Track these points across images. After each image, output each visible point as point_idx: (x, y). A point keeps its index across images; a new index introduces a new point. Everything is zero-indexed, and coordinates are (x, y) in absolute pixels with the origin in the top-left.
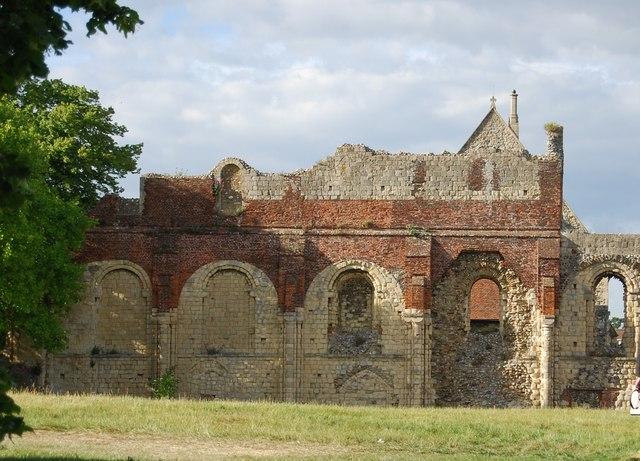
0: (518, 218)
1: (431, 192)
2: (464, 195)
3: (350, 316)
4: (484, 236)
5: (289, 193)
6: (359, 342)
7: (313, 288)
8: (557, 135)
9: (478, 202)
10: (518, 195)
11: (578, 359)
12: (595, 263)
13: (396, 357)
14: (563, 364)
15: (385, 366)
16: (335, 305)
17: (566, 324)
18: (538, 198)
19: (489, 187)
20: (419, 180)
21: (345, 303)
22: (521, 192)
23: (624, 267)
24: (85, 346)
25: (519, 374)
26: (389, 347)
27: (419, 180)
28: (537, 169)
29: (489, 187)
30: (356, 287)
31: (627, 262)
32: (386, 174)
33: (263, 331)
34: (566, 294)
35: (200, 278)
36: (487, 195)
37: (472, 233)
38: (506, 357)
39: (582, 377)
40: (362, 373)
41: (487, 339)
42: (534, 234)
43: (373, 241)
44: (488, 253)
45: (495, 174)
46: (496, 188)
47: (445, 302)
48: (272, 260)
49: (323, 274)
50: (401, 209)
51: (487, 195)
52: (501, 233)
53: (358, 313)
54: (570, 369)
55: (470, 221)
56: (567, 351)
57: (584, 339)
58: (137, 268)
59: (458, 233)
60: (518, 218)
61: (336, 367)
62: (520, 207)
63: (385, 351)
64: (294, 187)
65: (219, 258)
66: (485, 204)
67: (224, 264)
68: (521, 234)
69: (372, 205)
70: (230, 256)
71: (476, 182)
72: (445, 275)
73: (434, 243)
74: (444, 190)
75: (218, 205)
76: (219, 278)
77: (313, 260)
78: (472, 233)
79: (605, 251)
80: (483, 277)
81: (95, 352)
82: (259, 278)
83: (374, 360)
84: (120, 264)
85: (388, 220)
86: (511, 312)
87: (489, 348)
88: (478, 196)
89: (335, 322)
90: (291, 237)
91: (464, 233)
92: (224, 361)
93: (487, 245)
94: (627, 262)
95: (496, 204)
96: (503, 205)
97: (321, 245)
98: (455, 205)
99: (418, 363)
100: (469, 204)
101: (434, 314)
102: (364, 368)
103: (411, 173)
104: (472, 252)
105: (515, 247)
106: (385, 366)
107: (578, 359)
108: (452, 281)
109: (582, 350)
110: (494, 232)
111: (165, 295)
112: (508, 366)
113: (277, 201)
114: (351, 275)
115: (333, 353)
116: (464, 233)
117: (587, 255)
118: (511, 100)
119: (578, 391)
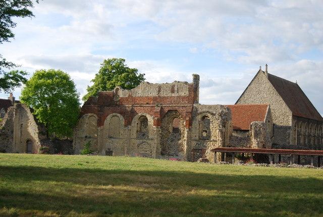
1: (163, 94)
2: (170, 95)
4: (174, 106)
6: (144, 135)
7: (133, 121)
8: (196, 78)
10: (183, 94)
12: (201, 113)
13: (152, 139)
15: (149, 142)
16: (139, 125)
17: (193, 130)
19: (176, 92)
20: (159, 91)
24: (84, 136)
25: (181, 144)
26: (150, 137)
27: (159, 91)
28: (188, 87)
29: (176, 92)
30: (144, 120)
31: (209, 113)
33: (122, 132)
35: (109, 117)
36: (175, 95)
38: (179, 140)
41: (175, 134)
46: (178, 93)
47: (164, 124)
48: (123, 113)
49: (136, 117)
50: (155, 99)
51: (175, 95)
53: (146, 127)
54: (194, 144)
58: (95, 115)
61: (138, 141)
62: (184, 98)
63: (149, 138)
65: (113, 113)
67: (114, 114)
69: (148, 98)
70: (115, 112)
71: (173, 91)
72: (164, 117)
73: (162, 108)
74: (165, 93)
75: (114, 99)
76: (113, 118)
77: (133, 113)
79: (204, 110)
81: (86, 137)
82: (121, 118)
84: (92, 114)
85: (152, 102)
86: (181, 128)
87: (175, 137)
88: (173, 95)
89: (139, 129)
90: (128, 106)
92: (113, 140)
93: (174, 108)
94: (209, 113)
96: (179, 97)
97: (135, 109)
98: (167, 98)
99: (156, 141)
100: (171, 97)
101: (161, 127)
103: (157, 89)
104: (171, 110)
106: (149, 142)
108: (166, 118)
109: (197, 138)
111: (100, 123)
112: (180, 142)
115: (137, 138)
117: (200, 111)
118: (265, 67)
119: (196, 150)
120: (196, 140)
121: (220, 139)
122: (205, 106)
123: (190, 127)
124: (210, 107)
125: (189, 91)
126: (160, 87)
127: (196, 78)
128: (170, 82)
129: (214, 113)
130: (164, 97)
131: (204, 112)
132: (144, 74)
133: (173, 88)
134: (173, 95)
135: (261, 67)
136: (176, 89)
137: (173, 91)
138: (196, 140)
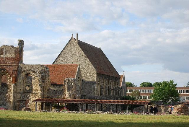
0: (10, 61)
8: (21, 43)
10: (10, 56)
11: (21, 93)
12: (25, 71)
14: (18, 94)
17: (18, 85)
18: (14, 57)
19: (4, 54)
22: (11, 55)
23: (31, 72)
25: (9, 97)
28: (14, 50)
29: (4, 54)
31: (32, 71)
34: (19, 78)
38: (7, 93)
39: (21, 97)
41: (4, 89)
42: (12, 65)
44: (4, 69)
46: (6, 54)
52: (6, 65)
54: (19, 96)
56: (19, 91)
57: (22, 88)
60: (10, 61)
62: (10, 59)
66: (3, 58)
68: (10, 65)
79: (27, 68)
86: (8, 83)
93: (3, 67)
94: (32, 71)
95: (6, 58)
96: (7, 58)
107: (21, 93)
109: (22, 91)
112: (7, 94)
117: (24, 69)
118: (76, 35)
120: (20, 93)
121: (40, 92)
122: (28, 65)
123: (16, 82)
124: (32, 66)
125: (15, 53)
127: (21, 43)
129: (36, 71)
131: (27, 70)
135: (72, 35)
136: (4, 52)
138: (20, 93)
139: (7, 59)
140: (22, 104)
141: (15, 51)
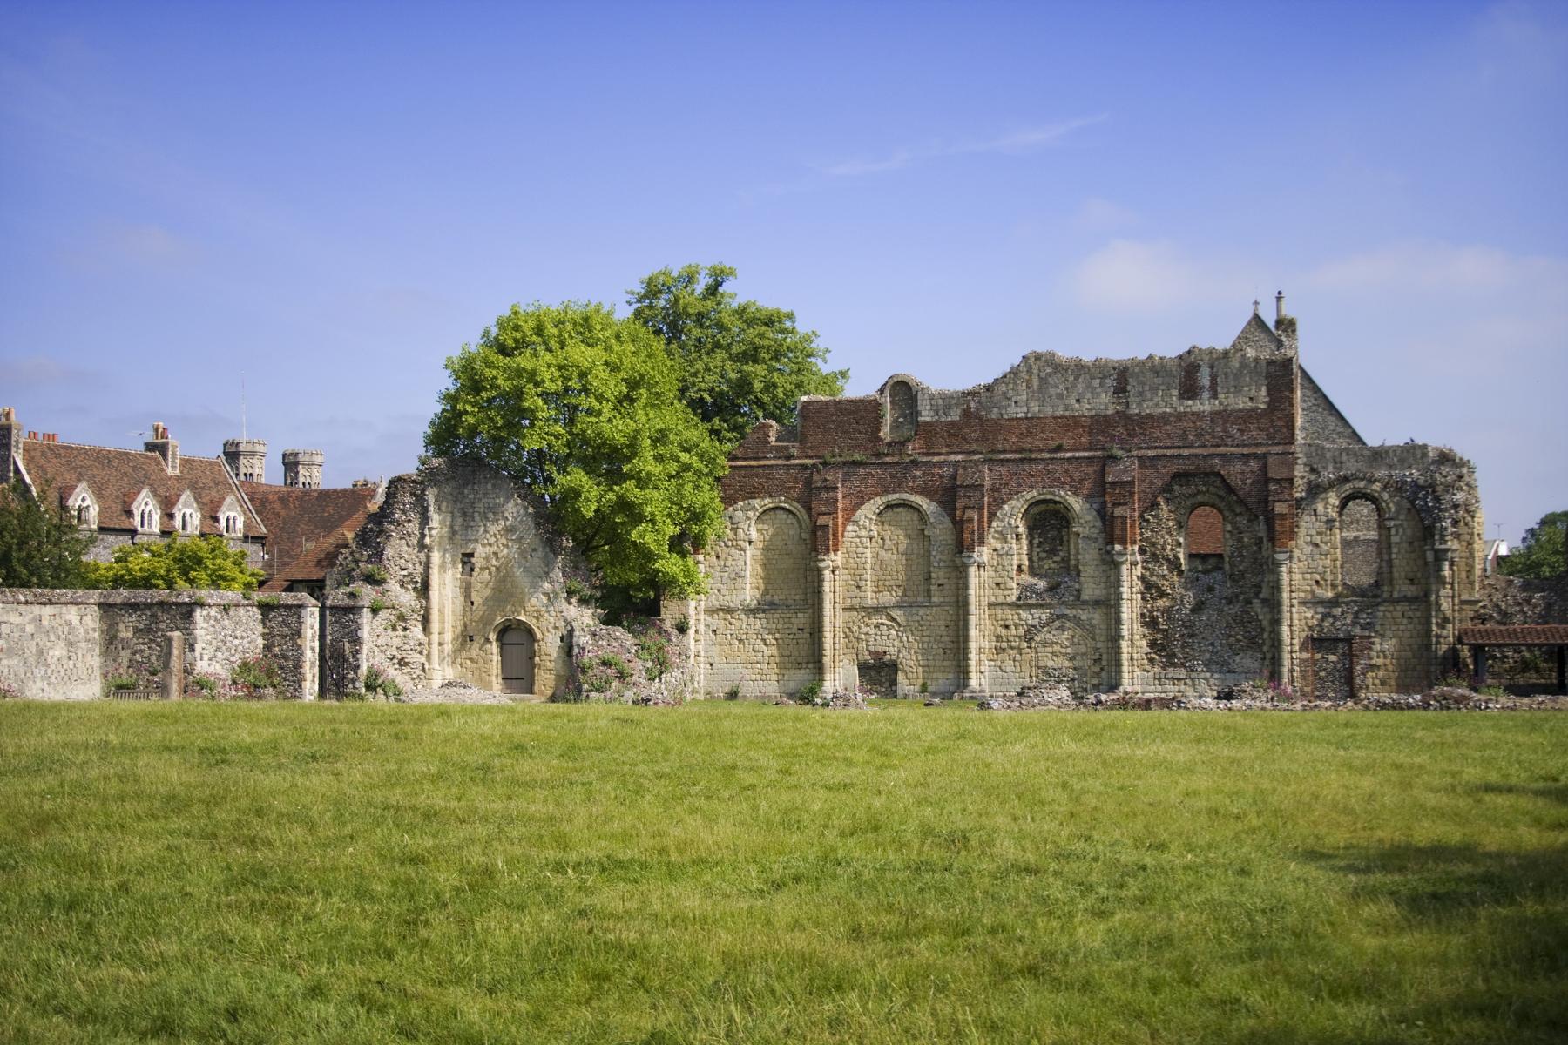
3: (1043, 555)
5: (967, 413)
9: (1193, 414)
10: (1242, 403)
15: (1083, 616)
19: (1206, 395)
20: (1120, 390)
21: (1036, 541)
29: (1206, 395)
32: (1080, 386)
36: (1204, 405)
37: (1186, 452)
40: (1057, 623)
43: (1066, 466)
44: (1206, 474)
45: (1213, 379)
46: (1215, 396)
50: (1100, 423)
51: (1204, 405)
52: (1222, 450)
55: (1184, 436)
59: (1169, 452)
62: (1246, 417)
63: (1085, 597)
64: (972, 405)
67: (892, 497)
68: (1246, 451)
71: (1190, 390)
78: (1186, 452)
80: (1202, 504)
83: (1073, 607)
87: (1211, 590)
88: (1195, 406)
91: (1176, 452)
95: (1215, 415)
96: (1221, 416)
98: (1163, 419)
100: (1180, 417)
102: (1058, 617)
105: (1238, 466)
110: (1212, 450)
113: (952, 423)
114: (1043, 507)
116: (1176, 452)
126: (1122, 377)
128: (1170, 348)
130: (1151, 416)
131: (1355, 477)
132: (827, 350)
133: (1189, 373)
134: (1195, 406)
136: (1204, 378)
137: (1190, 390)
139: (1225, 422)
140: (1333, 658)
141: (1268, 376)
